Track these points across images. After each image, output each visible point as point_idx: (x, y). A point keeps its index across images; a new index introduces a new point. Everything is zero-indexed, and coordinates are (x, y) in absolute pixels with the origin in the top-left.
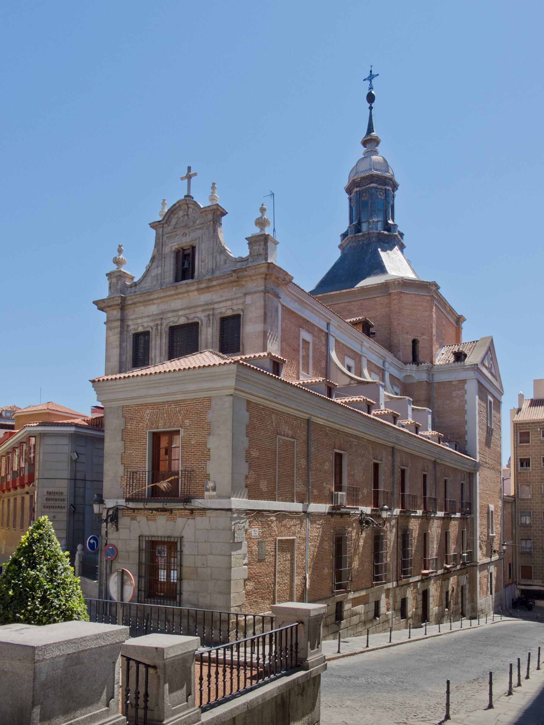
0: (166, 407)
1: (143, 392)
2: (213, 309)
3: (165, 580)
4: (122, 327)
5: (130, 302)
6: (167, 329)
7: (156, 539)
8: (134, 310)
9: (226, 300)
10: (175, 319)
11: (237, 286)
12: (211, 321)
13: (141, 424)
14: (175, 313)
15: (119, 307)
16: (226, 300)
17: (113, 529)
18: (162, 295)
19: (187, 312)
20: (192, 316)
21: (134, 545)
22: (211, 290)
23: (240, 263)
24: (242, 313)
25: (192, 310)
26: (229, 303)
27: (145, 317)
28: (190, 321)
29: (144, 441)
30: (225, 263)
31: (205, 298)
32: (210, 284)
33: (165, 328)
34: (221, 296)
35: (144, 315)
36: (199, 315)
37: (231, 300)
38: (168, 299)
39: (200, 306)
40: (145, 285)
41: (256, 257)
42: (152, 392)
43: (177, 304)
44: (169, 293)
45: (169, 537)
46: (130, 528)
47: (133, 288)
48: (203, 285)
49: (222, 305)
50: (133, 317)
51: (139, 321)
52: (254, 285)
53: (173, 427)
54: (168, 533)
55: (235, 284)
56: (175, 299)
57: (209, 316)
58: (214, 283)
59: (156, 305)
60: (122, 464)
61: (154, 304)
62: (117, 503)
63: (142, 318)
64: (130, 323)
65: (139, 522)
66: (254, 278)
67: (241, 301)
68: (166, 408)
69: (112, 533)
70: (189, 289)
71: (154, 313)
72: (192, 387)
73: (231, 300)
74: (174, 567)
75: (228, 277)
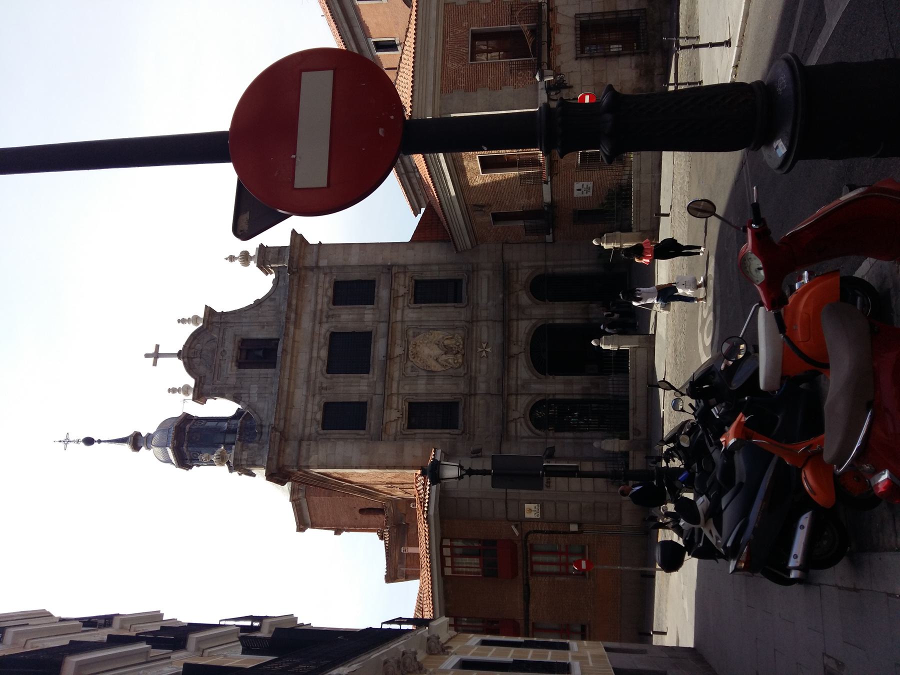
0: (448, 46)
1: (431, 63)
2: (321, 311)
3: (620, 46)
4: (309, 439)
5: (282, 423)
6: (329, 375)
7: (578, 42)
8: (293, 425)
9: (317, 294)
10: (320, 363)
11: (303, 281)
12: (336, 313)
13: (462, 72)
14: (314, 363)
15: (283, 442)
16: (317, 294)
17: (570, 93)
18: (287, 374)
19: (316, 345)
20: (322, 340)
21: (586, 65)
22: (299, 311)
23: (279, 283)
24: (335, 277)
25: (316, 338)
26: (320, 292)
27: (306, 407)
28: (328, 342)
29: (479, 67)
30: (274, 299)
31: (306, 322)
32: (294, 307)
33: (326, 378)
34: (310, 301)
35: (303, 408)
36: (323, 331)
37: (317, 287)
38: (293, 369)
39: (314, 325)
40: (265, 412)
41: (281, 256)
42: (432, 54)
43: (303, 359)
44: (288, 364)
45: (576, 28)
46: (569, 73)
47: (263, 430)
48: (293, 316)
49: (320, 301)
50: (301, 426)
51: (309, 417)
52: (309, 257)
53: (468, 37)
54: (572, 31)
55: (301, 282)
56: (296, 362)
57: (328, 317)
58: (294, 302)
59: (296, 390)
60: (501, 89)
61: (293, 393)
62: (542, 89)
63: (306, 411)
64: (307, 431)
65: (562, 63)
66: (302, 254)
67: (322, 276)
68: (448, 46)
69: (575, 93)
70: (291, 336)
71: (304, 393)
72: (434, 13)
73: (317, 287)
74: (607, 49)
75: (293, 285)
